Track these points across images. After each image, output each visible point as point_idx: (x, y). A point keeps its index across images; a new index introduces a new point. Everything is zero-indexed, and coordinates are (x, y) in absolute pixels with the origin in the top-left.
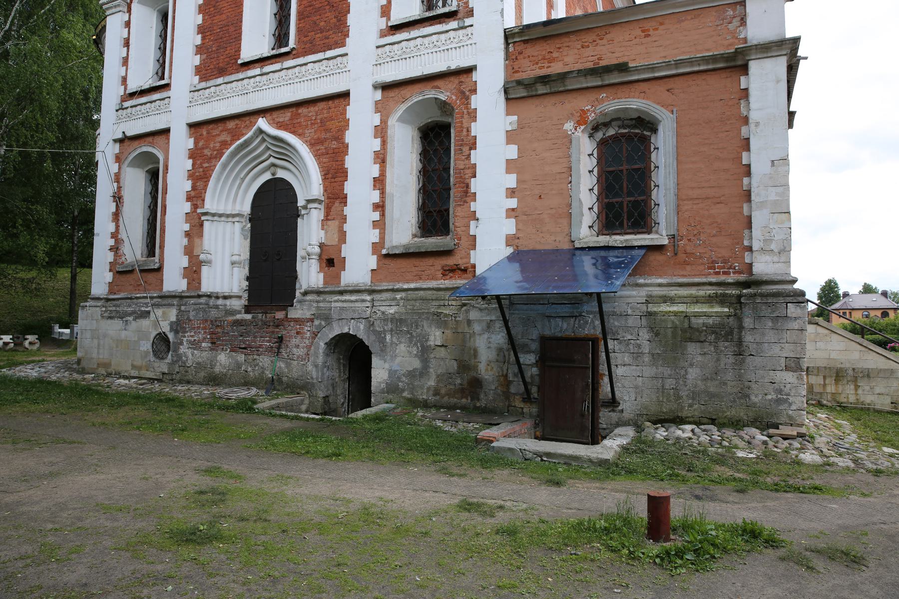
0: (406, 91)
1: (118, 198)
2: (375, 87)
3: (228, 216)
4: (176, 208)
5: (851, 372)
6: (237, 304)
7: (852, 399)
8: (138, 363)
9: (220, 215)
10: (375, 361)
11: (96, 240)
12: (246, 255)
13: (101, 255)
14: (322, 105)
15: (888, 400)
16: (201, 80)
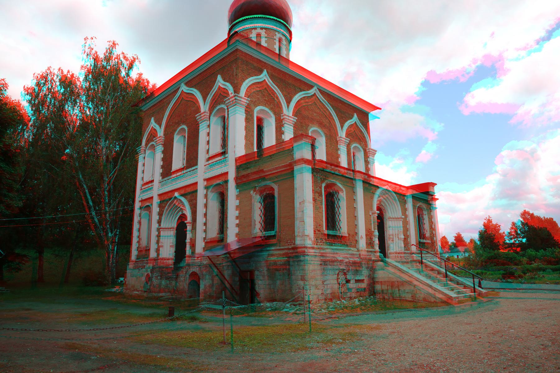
1: (140, 223)
2: (205, 180)
4: (155, 225)
6: (171, 262)
12: (175, 243)
15: (410, 296)
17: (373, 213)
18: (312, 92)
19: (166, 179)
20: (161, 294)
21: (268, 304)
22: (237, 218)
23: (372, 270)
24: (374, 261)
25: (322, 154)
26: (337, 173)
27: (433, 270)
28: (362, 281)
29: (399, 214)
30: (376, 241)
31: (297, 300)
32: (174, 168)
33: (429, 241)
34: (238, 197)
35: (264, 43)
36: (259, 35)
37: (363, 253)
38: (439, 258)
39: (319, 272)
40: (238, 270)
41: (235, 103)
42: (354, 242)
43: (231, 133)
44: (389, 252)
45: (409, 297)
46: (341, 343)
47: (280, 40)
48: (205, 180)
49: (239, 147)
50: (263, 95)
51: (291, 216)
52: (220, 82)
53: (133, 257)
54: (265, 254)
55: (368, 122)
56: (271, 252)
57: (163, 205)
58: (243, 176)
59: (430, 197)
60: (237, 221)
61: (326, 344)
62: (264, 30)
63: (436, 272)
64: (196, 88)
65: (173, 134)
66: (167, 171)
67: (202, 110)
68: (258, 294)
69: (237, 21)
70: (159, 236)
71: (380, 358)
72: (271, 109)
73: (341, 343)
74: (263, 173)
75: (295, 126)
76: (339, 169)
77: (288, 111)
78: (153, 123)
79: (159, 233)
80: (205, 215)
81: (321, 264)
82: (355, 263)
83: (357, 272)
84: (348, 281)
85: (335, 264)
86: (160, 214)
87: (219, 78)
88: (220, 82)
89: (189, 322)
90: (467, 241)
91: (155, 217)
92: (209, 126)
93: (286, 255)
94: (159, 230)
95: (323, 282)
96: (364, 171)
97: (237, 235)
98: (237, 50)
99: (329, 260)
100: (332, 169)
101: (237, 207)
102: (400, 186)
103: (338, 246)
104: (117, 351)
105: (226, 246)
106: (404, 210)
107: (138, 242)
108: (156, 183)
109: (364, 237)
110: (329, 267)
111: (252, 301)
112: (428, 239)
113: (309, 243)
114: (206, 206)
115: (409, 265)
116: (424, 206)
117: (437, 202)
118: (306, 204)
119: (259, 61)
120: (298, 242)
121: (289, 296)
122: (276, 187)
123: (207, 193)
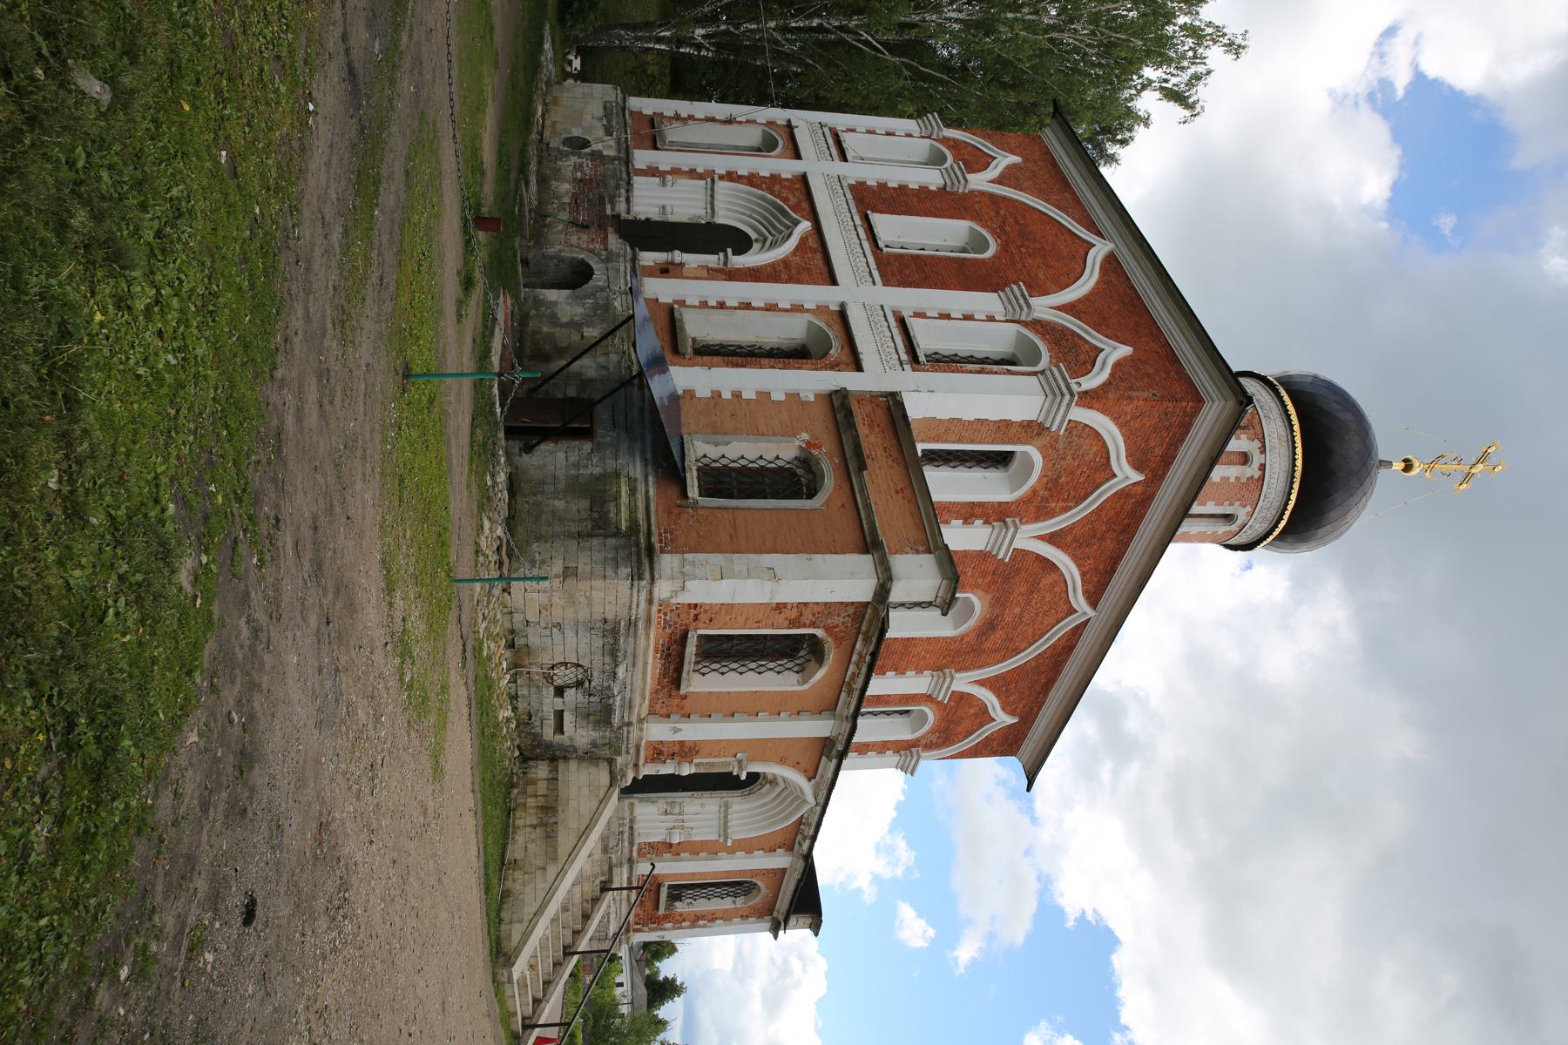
0: (838, 327)
1: (730, 121)
3: (712, 204)
5: (552, 820)
6: (621, 207)
7: (519, 822)
8: (559, 127)
9: (712, 196)
10: (566, 292)
11: (686, 103)
12: (672, 219)
13: (668, 106)
14: (825, 269)
15: (519, 856)
16: (852, 187)
17: (740, 762)
18: (1079, 602)
19: (849, 196)
20: (533, 179)
21: (502, 477)
22: (737, 395)
23: (590, 757)
24: (611, 761)
25: (901, 626)
26: (852, 668)
27: (586, 917)
28: (560, 728)
29: (738, 832)
30: (667, 769)
31: (512, 552)
32: (877, 219)
33: (661, 911)
34: (793, 397)
35: (1218, 473)
36: (1245, 459)
38: (616, 935)
39: (584, 615)
40: (597, 397)
41: (1054, 393)
42: (664, 711)
44: (636, 802)
45: (515, 851)
46: (401, 680)
47: (1228, 518)
49: (932, 401)
50: (1076, 467)
51: (738, 542)
52: (1116, 352)
53: (635, 103)
54: (637, 470)
56: (641, 487)
57: (777, 187)
58: (849, 414)
59: (781, 918)
60: (727, 395)
61: (401, 640)
62: (1257, 474)
63: (579, 927)
64: (1097, 283)
65: (972, 219)
66: (871, 200)
67: (1034, 301)
68: (528, 449)
69: (1286, 398)
70: (692, 174)
71: (364, 780)
72: (1034, 491)
73: (401, 680)
74: (859, 469)
75: (983, 556)
76: (862, 677)
77: (1028, 538)
78: (1005, 160)
79: (701, 177)
80: (747, 306)
81: (606, 621)
82: (608, 711)
83: (584, 715)
84: (560, 691)
85: (608, 660)
86: (752, 180)
87: (1124, 351)
88: (1116, 352)
89: (459, 273)
90: (663, 1012)
91: (745, 165)
92: (991, 319)
93: (634, 527)
94: (709, 176)
95: (559, 625)
96: (855, 739)
97: (690, 393)
98: (1199, 401)
99: (616, 640)
100: (860, 655)
101: (764, 396)
102: (814, 838)
103: (654, 667)
104: (390, 100)
105: (659, 364)
106: (748, 846)
107: (677, 117)
108: (839, 167)
109: (679, 737)
110: (598, 643)
111: (511, 432)
112: (667, 908)
113: (663, 589)
114: (771, 308)
115: (598, 855)
116: (756, 900)
117: (769, 935)
118: (769, 585)
119: (1167, 461)
120: (667, 562)
122: (817, 502)
123: (808, 311)
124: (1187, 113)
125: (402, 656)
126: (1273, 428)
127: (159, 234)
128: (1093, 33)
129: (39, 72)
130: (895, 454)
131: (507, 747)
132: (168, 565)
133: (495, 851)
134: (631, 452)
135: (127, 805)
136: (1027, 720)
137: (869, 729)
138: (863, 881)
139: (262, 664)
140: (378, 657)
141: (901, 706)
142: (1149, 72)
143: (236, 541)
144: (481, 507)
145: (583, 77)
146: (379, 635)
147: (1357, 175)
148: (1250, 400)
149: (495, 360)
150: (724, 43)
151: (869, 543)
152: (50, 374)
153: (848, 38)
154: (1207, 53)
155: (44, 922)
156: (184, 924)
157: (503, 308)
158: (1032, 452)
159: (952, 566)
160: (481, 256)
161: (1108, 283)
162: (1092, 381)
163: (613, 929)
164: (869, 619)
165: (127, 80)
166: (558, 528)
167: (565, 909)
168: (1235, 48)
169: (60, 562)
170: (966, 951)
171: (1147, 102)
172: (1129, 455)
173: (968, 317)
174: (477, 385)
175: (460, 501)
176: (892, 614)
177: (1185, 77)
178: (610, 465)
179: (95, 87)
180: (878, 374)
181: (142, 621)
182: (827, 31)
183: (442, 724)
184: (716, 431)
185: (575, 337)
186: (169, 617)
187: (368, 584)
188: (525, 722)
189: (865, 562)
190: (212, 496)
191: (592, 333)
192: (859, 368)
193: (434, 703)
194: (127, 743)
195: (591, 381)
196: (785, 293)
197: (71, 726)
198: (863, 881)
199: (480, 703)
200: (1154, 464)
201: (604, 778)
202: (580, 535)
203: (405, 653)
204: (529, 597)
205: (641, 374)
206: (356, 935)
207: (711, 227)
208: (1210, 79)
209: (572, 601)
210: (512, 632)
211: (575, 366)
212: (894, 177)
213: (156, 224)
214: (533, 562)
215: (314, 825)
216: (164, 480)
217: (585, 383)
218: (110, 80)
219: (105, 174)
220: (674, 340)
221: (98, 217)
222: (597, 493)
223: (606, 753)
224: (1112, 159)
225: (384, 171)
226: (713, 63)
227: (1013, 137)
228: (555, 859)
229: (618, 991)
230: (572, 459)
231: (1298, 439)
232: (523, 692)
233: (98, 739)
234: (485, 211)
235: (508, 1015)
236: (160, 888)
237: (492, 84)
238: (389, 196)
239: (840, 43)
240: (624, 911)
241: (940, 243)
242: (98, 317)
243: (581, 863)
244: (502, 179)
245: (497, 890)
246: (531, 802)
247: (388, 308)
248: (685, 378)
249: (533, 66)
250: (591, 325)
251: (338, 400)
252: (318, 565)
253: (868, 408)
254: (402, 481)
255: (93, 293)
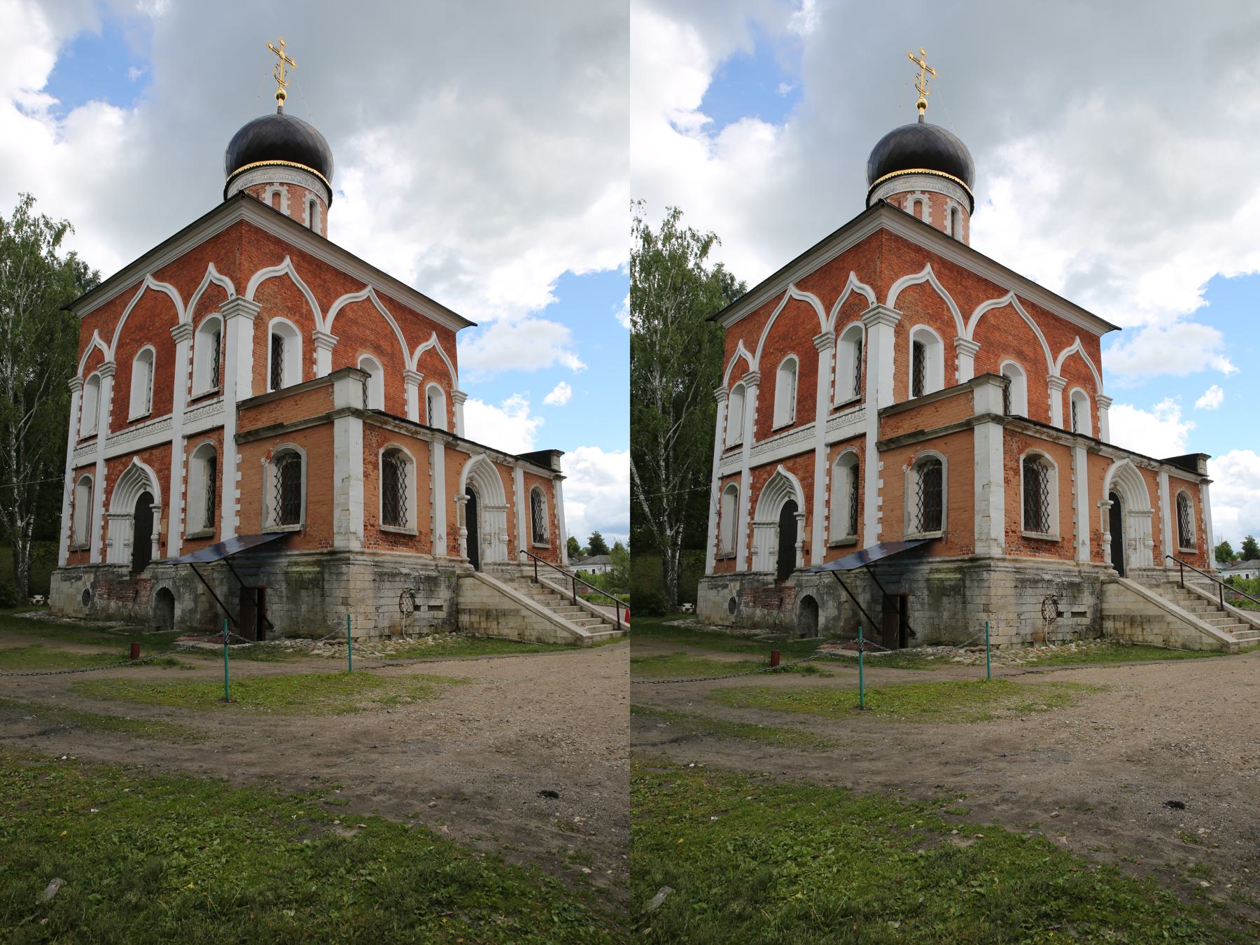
18: (363, 294)
20: (109, 624)
22: (238, 501)
25: (377, 402)
27: (553, 592)
28: (439, 608)
31: (333, 636)
32: (132, 416)
34: (239, 467)
35: (285, 211)
36: (276, 195)
37: (442, 563)
38: (564, 574)
39: (370, 593)
40: (239, 585)
43: (229, 359)
45: (513, 635)
47: (312, 205)
48: (184, 437)
50: (282, 297)
51: (327, 500)
53: (62, 562)
54: (283, 561)
55: (455, 346)
56: (294, 559)
58: (249, 433)
60: (238, 507)
62: (286, 187)
65: (132, 359)
67: (182, 322)
68: (271, 626)
69: (240, 170)
72: (296, 322)
74: (282, 428)
75: (335, 352)
78: (97, 339)
79: (107, 523)
80: (185, 495)
82: (429, 579)
84: (417, 608)
87: (211, 267)
90: (609, 544)
91: (99, 496)
93: (318, 563)
94: (106, 518)
96: (446, 429)
97: (237, 529)
98: (242, 222)
99: (386, 574)
101: (239, 485)
102: (505, 455)
105: (219, 548)
106: (510, 495)
114: (186, 480)
115: (516, 585)
120: (339, 543)
121: (319, 629)
122: (303, 453)
124: (68, 229)
125: (395, 703)
126: (258, 177)
127: (141, 849)
128: (20, 286)
129: (43, 921)
130: (273, 406)
131: (450, 639)
132: (340, 844)
133: (513, 647)
134: (272, 565)
135: (486, 868)
136: (434, 326)
137: (440, 422)
138: (532, 425)
139: (400, 787)
140: (396, 717)
141: (425, 402)
142: (44, 253)
143: (326, 803)
144: (306, 655)
145: (46, 594)
146: (383, 717)
147: (106, 127)
148: (241, 192)
149: (217, 646)
150: (26, 509)
151: (328, 421)
152: (225, 915)
153: (23, 434)
154: (32, 217)
155: (556, 919)
156: (558, 834)
157: (185, 642)
158: (273, 323)
159: (341, 372)
160: (154, 655)
161: (171, 277)
162: (230, 287)
163: (560, 576)
164: (373, 421)
165: (48, 869)
166: (318, 609)
167: (548, 605)
168: (29, 201)
169: (339, 909)
170: (574, 363)
171: (62, 253)
172: (274, 264)
173: (191, 362)
174: (232, 657)
175: (302, 668)
176: (370, 407)
177: (46, 231)
178: (280, 577)
179: (52, 888)
180: (225, 416)
181: (375, 859)
182: (19, 447)
183: (436, 678)
184: (260, 513)
185: (203, 598)
186: (372, 843)
187: (352, 723)
188: (435, 628)
189: (339, 424)
190: (299, 817)
191: (201, 588)
192: (222, 427)
193: (424, 684)
194: (448, 868)
195: (230, 590)
196: (177, 472)
197: (438, 902)
198: (532, 425)
199: (424, 656)
200: (279, 249)
201: (469, 581)
202: (323, 596)
203: (394, 701)
204: (360, 626)
205: (225, 559)
206: (564, 731)
207: (136, 517)
208: (48, 216)
209: (362, 601)
210: (381, 636)
211: (221, 598)
212: (106, 406)
213: (135, 851)
214: (339, 624)
215: (497, 756)
216: (289, 846)
217: (231, 593)
218: (48, 879)
219: (105, 882)
220: (206, 538)
221: (131, 886)
222: (297, 585)
223: (454, 580)
224: (96, 275)
225: (103, 713)
226: (37, 515)
227: (83, 334)
228: (518, 611)
229: (597, 572)
230: (277, 600)
231: (265, 163)
232: (417, 630)
233: (446, 886)
234: (127, 653)
235: (612, 639)
236: (535, 849)
237: (50, 648)
238: (118, 710)
239: (26, 437)
240: (549, 569)
241: (146, 379)
242: (191, 886)
243: (520, 595)
244: (107, 642)
245: (536, 646)
246: (483, 625)
247: (185, 711)
248: (228, 532)
249: (40, 624)
250: (196, 588)
251: (242, 742)
252: (340, 753)
253: (246, 422)
254: (290, 703)
255: (177, 889)
